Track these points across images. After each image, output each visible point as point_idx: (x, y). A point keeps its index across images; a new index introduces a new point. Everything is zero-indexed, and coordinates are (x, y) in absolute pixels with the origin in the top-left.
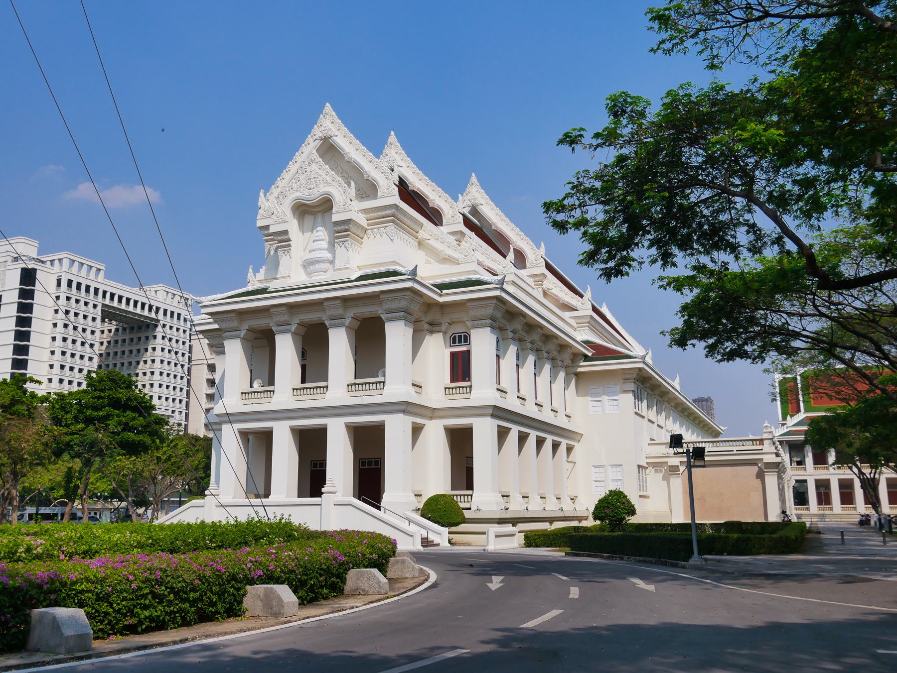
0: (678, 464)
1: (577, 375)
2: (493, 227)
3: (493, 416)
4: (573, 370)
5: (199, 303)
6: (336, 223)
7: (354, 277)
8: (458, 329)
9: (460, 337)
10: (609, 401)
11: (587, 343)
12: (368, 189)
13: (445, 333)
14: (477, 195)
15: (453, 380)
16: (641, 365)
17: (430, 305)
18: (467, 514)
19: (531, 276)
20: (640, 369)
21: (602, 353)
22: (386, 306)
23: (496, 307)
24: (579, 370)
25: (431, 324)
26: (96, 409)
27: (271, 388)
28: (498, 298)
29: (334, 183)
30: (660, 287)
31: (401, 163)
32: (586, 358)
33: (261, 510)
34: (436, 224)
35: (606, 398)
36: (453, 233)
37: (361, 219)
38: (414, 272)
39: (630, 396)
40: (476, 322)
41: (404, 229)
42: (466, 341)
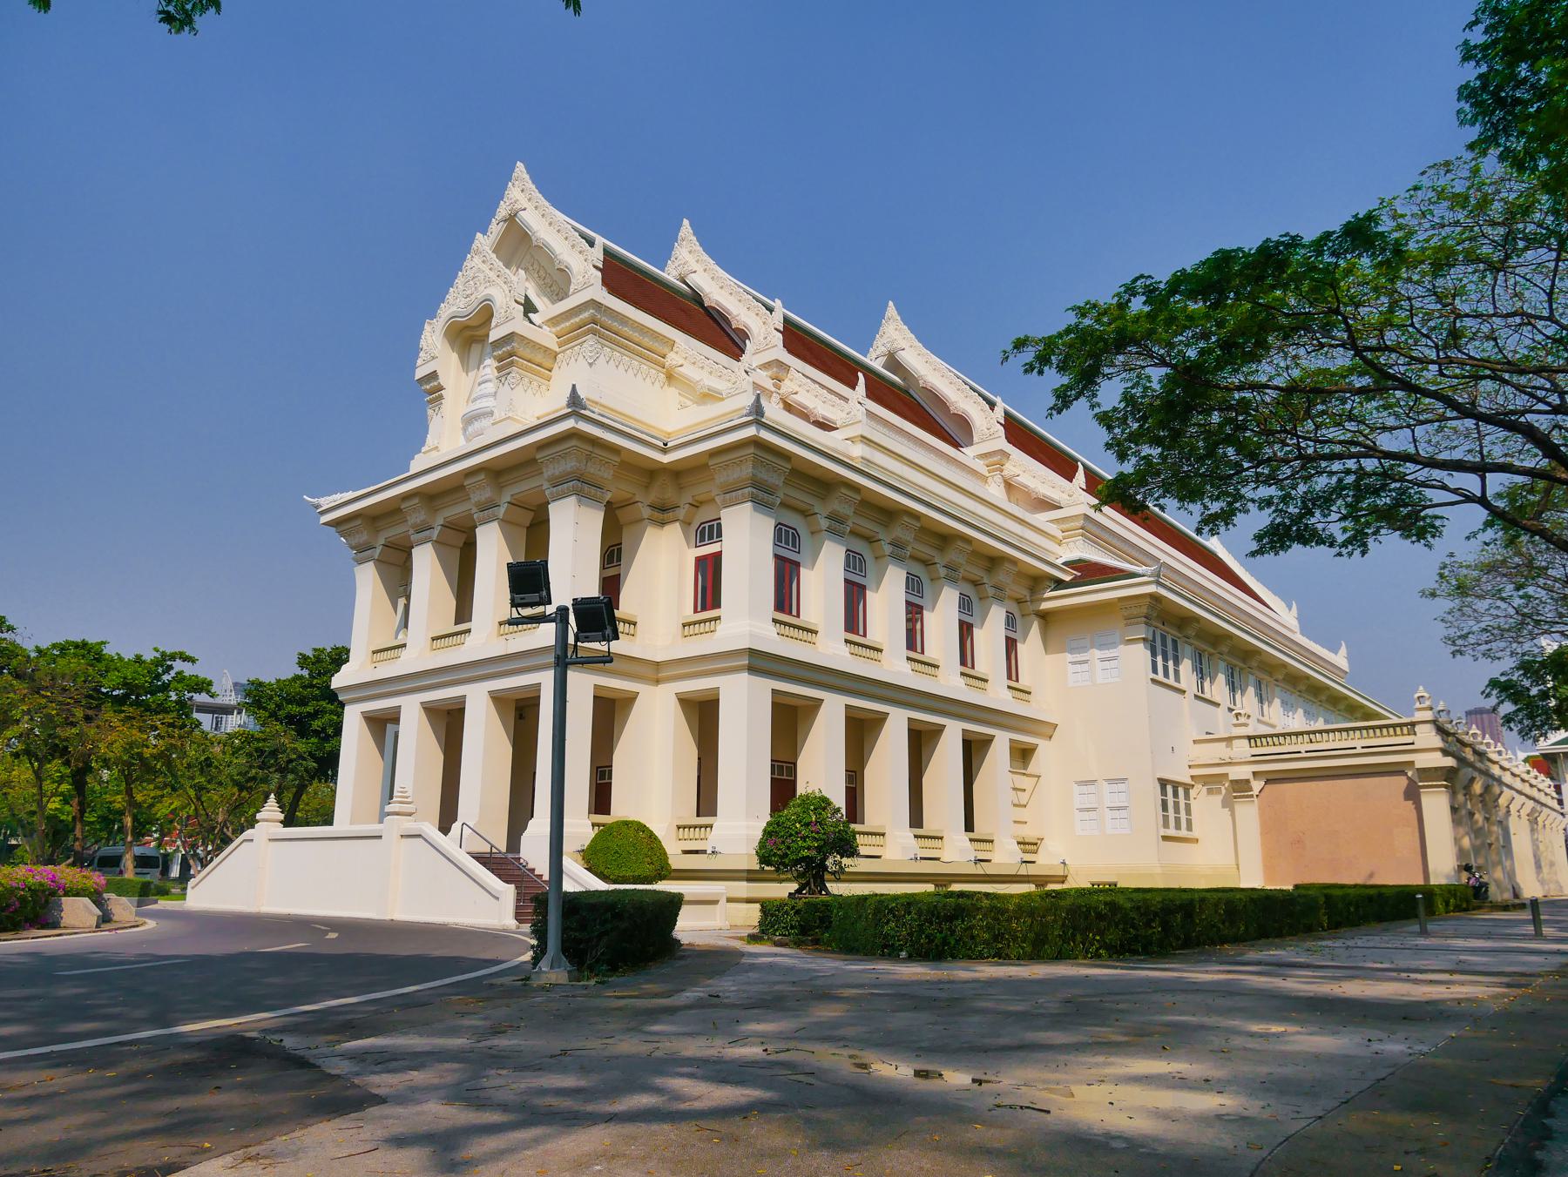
0: (1251, 777)
1: (1044, 617)
3: (752, 669)
4: (1031, 607)
5: (317, 507)
8: (704, 515)
9: (711, 527)
10: (1103, 660)
12: (557, 282)
13: (686, 524)
14: (895, 335)
15: (696, 611)
16: (1152, 589)
17: (650, 473)
20: (1155, 598)
21: (1089, 572)
23: (757, 462)
24: (1045, 606)
26: (303, 702)
28: (756, 442)
29: (499, 281)
30: (1029, 368)
31: (695, 267)
32: (1060, 584)
35: (1096, 654)
36: (766, 366)
37: (547, 337)
38: (575, 400)
39: (1140, 653)
42: (720, 535)
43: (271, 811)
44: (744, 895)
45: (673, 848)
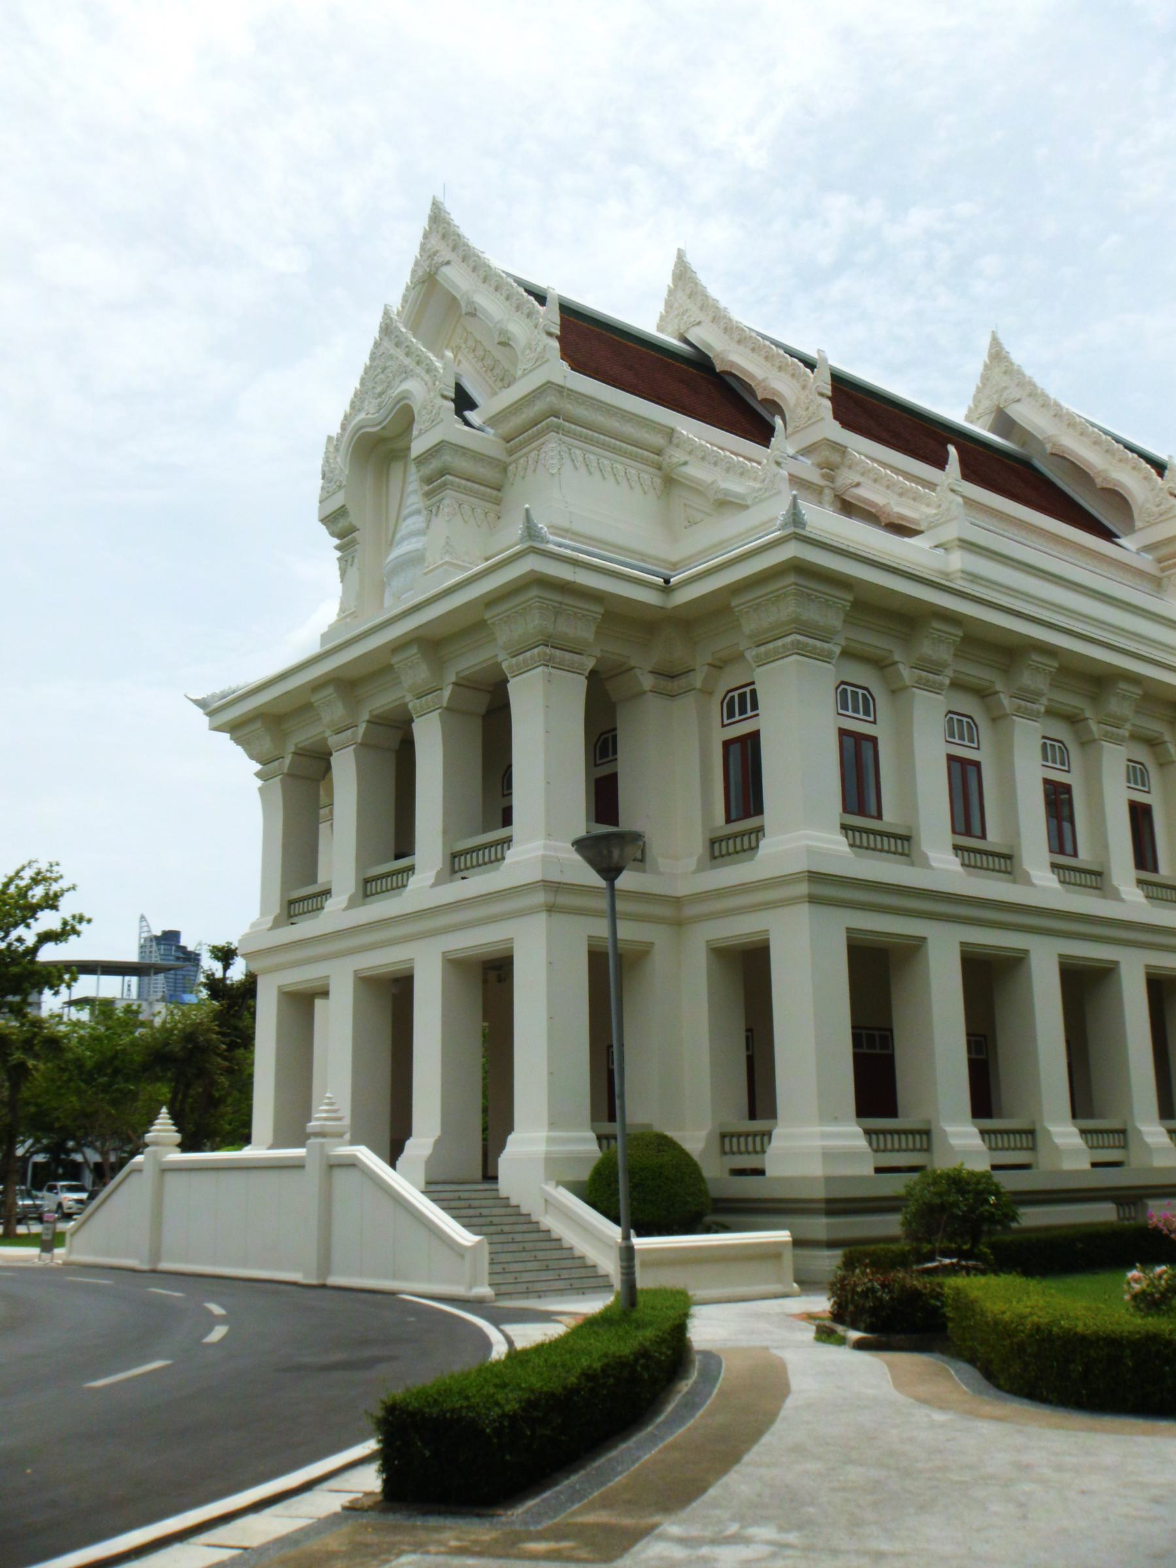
2: (1049, 447)
6: (422, 460)
9: (742, 697)
15: (728, 820)
22: (505, 635)
28: (798, 568)
29: (419, 370)
43: (163, 1128)
44: (822, 1235)
45: (714, 1171)
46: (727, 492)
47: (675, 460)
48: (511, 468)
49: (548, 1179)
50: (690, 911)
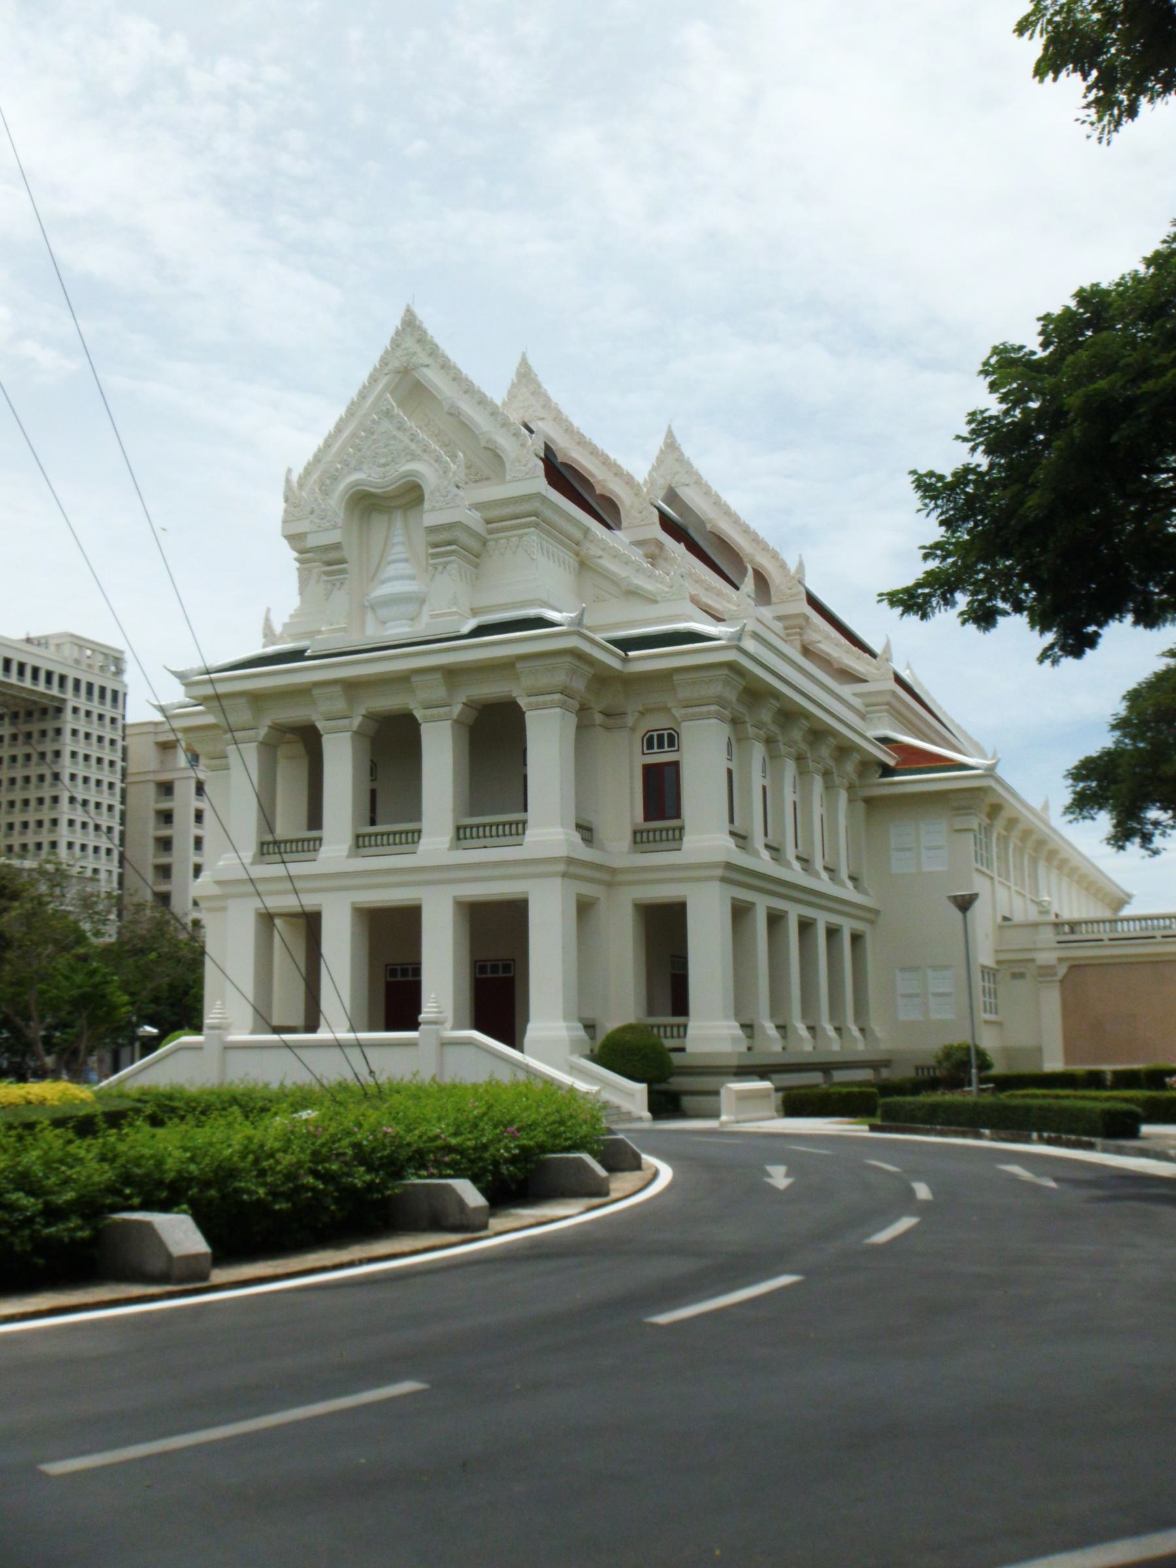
2: (709, 527)
6: (431, 530)
7: (466, 629)
8: (657, 722)
9: (660, 737)
11: (885, 740)
15: (647, 818)
17: (603, 679)
18: (676, 1059)
19: (779, 618)
22: (528, 682)
25: (607, 714)
27: (314, 834)
28: (732, 666)
29: (426, 456)
33: (355, 1055)
34: (609, 527)
36: (639, 543)
40: (690, 710)
41: (549, 534)
42: (671, 744)
46: (638, 587)
47: (592, 553)
48: (491, 544)
49: (572, 1052)
50: (621, 878)
